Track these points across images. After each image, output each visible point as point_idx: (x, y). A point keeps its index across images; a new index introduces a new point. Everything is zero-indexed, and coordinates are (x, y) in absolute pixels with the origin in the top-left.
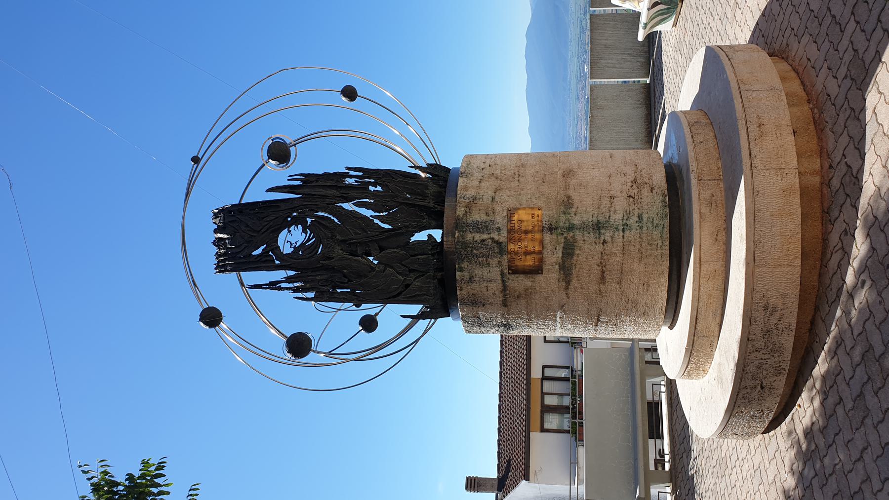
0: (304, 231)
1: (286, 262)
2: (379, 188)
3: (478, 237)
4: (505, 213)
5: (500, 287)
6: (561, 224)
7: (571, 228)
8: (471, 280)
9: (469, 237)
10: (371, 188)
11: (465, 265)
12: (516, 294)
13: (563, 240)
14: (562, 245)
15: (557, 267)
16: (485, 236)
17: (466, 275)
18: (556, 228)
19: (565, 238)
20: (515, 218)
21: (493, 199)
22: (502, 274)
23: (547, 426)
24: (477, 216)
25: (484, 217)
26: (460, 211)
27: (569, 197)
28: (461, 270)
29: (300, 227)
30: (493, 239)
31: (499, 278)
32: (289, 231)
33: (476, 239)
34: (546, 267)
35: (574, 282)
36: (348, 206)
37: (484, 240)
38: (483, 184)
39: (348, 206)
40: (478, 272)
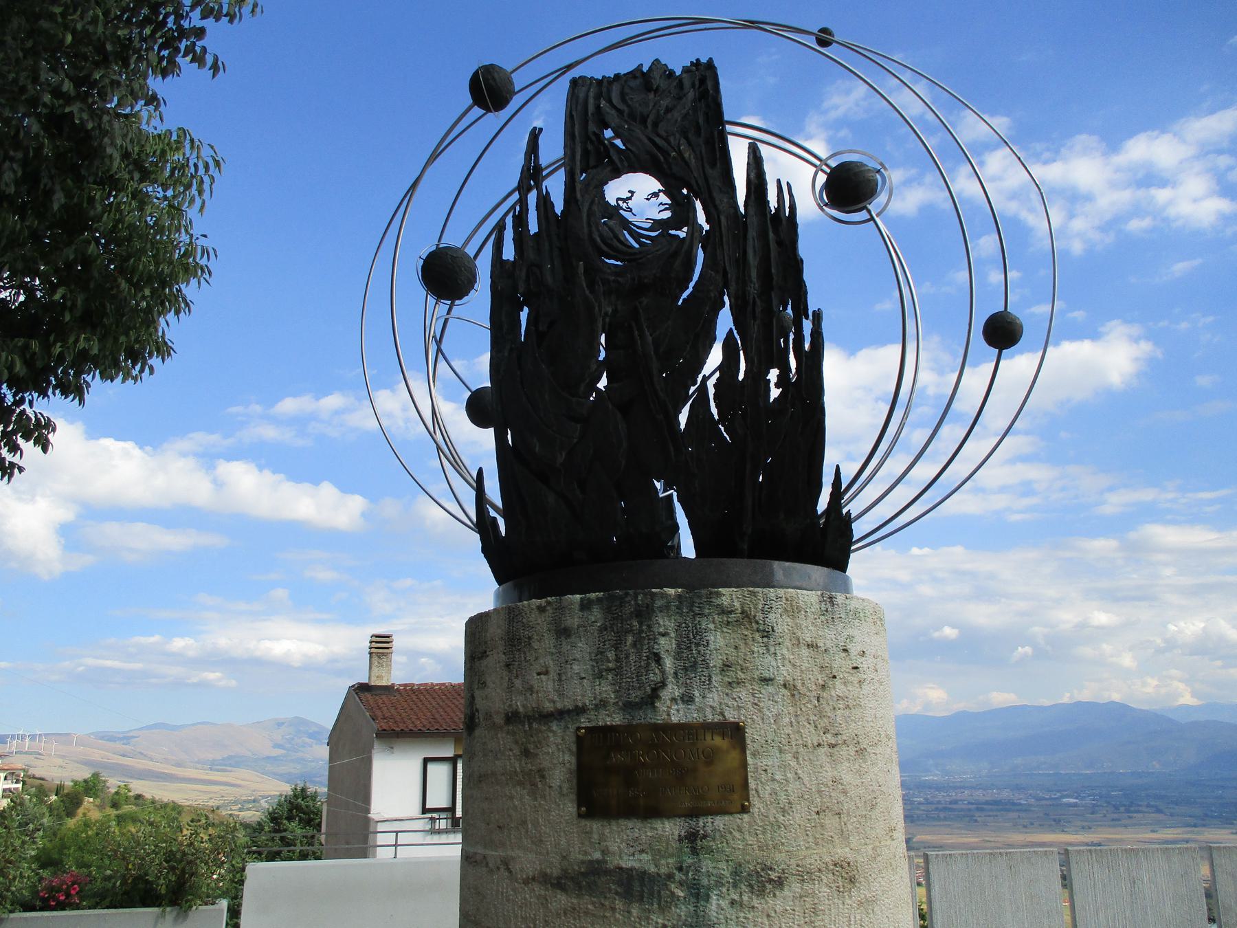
0: (657, 224)
1: (586, 193)
2: (775, 393)
3: (666, 645)
4: (731, 716)
5: (548, 706)
6: (707, 865)
7: (698, 894)
8: (563, 633)
9: (665, 623)
10: (773, 375)
11: (596, 614)
12: (531, 747)
13: (663, 870)
14: (653, 869)
15: (597, 855)
16: (668, 663)
17: (573, 620)
18: (695, 852)
19: (670, 877)
20: (718, 741)
21: (766, 681)
22: (580, 710)
23: (430, 767)
24: (718, 642)
25: (715, 661)
26: (729, 596)
27: (780, 883)
28: (585, 606)
29: (667, 215)
30: (663, 684)
31: (568, 704)
32: (656, 195)
33: (662, 641)
34: (595, 826)
35: (561, 900)
36: (725, 321)
37: (658, 659)
38: (805, 652)
39: (725, 321)
40: (582, 648)
